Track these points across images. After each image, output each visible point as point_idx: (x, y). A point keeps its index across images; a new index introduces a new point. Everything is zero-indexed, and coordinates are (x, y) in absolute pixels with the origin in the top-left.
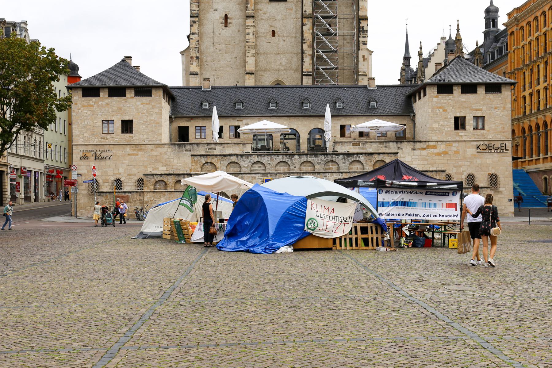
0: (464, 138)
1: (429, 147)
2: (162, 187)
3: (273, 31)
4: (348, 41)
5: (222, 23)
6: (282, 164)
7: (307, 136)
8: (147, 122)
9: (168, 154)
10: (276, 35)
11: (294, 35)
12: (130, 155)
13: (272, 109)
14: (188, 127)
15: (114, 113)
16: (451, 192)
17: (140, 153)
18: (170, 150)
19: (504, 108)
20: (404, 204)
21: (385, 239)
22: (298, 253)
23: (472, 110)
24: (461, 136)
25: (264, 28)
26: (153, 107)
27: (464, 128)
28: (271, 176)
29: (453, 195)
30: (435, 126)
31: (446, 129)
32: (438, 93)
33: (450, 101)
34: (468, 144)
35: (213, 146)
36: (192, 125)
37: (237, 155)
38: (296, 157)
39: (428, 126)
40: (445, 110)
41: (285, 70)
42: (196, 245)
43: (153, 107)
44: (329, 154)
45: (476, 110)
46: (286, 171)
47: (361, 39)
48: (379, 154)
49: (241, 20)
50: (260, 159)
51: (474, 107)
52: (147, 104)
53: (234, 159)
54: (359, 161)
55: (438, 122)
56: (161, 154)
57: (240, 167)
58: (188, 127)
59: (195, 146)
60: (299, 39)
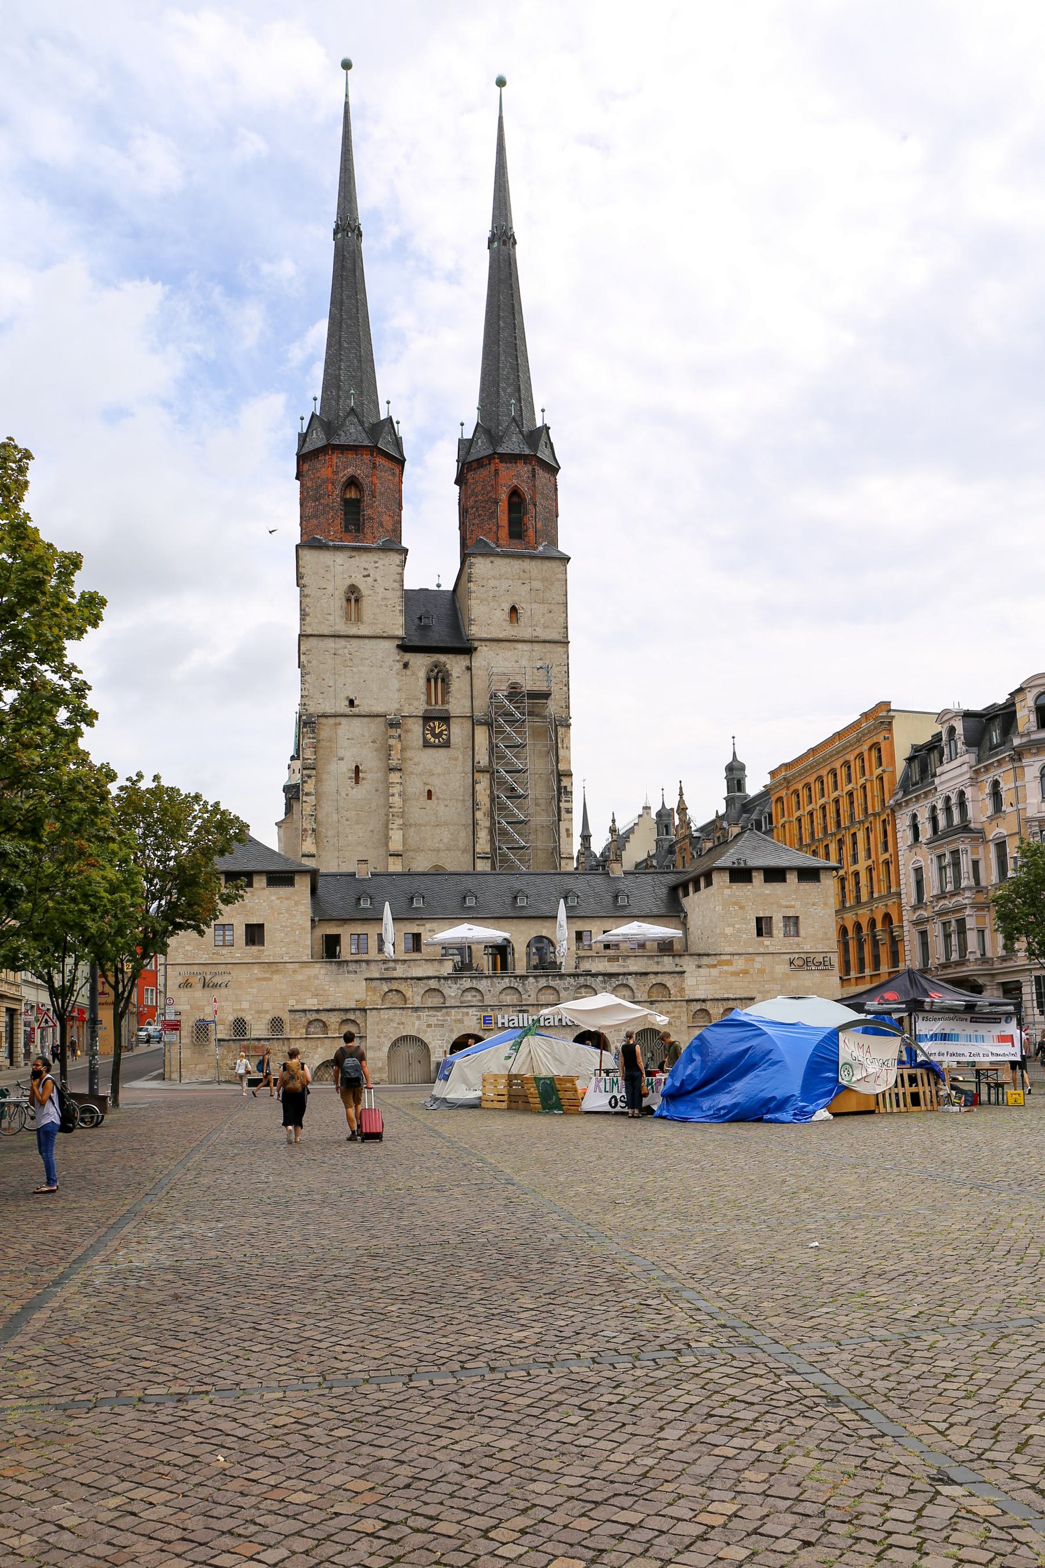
0: (771, 950)
1: (720, 963)
2: (318, 1030)
3: (429, 792)
4: (543, 807)
5: (350, 778)
6: (509, 991)
7: (524, 949)
8: (286, 927)
9: (321, 977)
10: (433, 797)
11: (461, 798)
12: (258, 979)
13: (470, 908)
14: (339, 935)
15: (234, 913)
16: (1003, 1017)
17: (275, 977)
18: (323, 971)
19: (825, 904)
20: (945, 1037)
21: (941, 1093)
22: (837, 1119)
23: (781, 906)
25: (416, 787)
26: (296, 904)
27: (770, 934)
28: (492, 1010)
29: (1006, 1022)
30: (729, 931)
31: (744, 936)
34: (777, 958)
35: (392, 964)
36: (346, 932)
37: (439, 978)
38: (531, 980)
39: (718, 931)
40: (742, 908)
41: (448, 849)
42: (593, 1117)
43: (296, 904)
44: (582, 975)
45: (787, 907)
46: (515, 1002)
47: (563, 805)
48: (656, 973)
49: (379, 774)
50: (474, 983)
52: (286, 899)
53: (433, 984)
54: (626, 986)
56: (309, 978)
57: (444, 997)
58: (339, 935)
59: (364, 964)
60: (469, 804)
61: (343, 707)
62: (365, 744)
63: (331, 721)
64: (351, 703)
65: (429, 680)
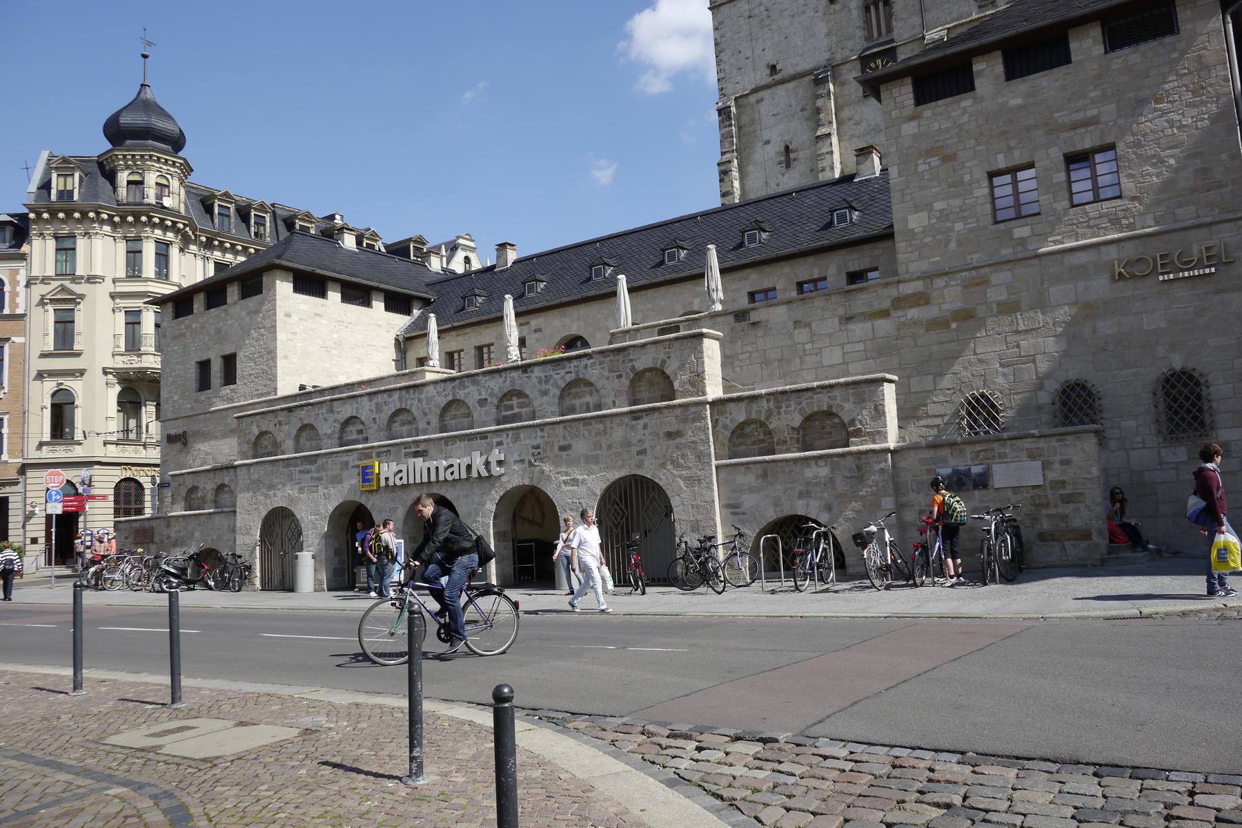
5: (780, 163)
24: (1023, 241)
31: (959, 226)
32: (919, 102)
33: (966, 118)
45: (1074, 126)
51: (1062, 117)
55: (928, 207)
61: (763, 76)
62: (793, 116)
63: (753, 98)
64: (773, 69)
65: (867, 9)
